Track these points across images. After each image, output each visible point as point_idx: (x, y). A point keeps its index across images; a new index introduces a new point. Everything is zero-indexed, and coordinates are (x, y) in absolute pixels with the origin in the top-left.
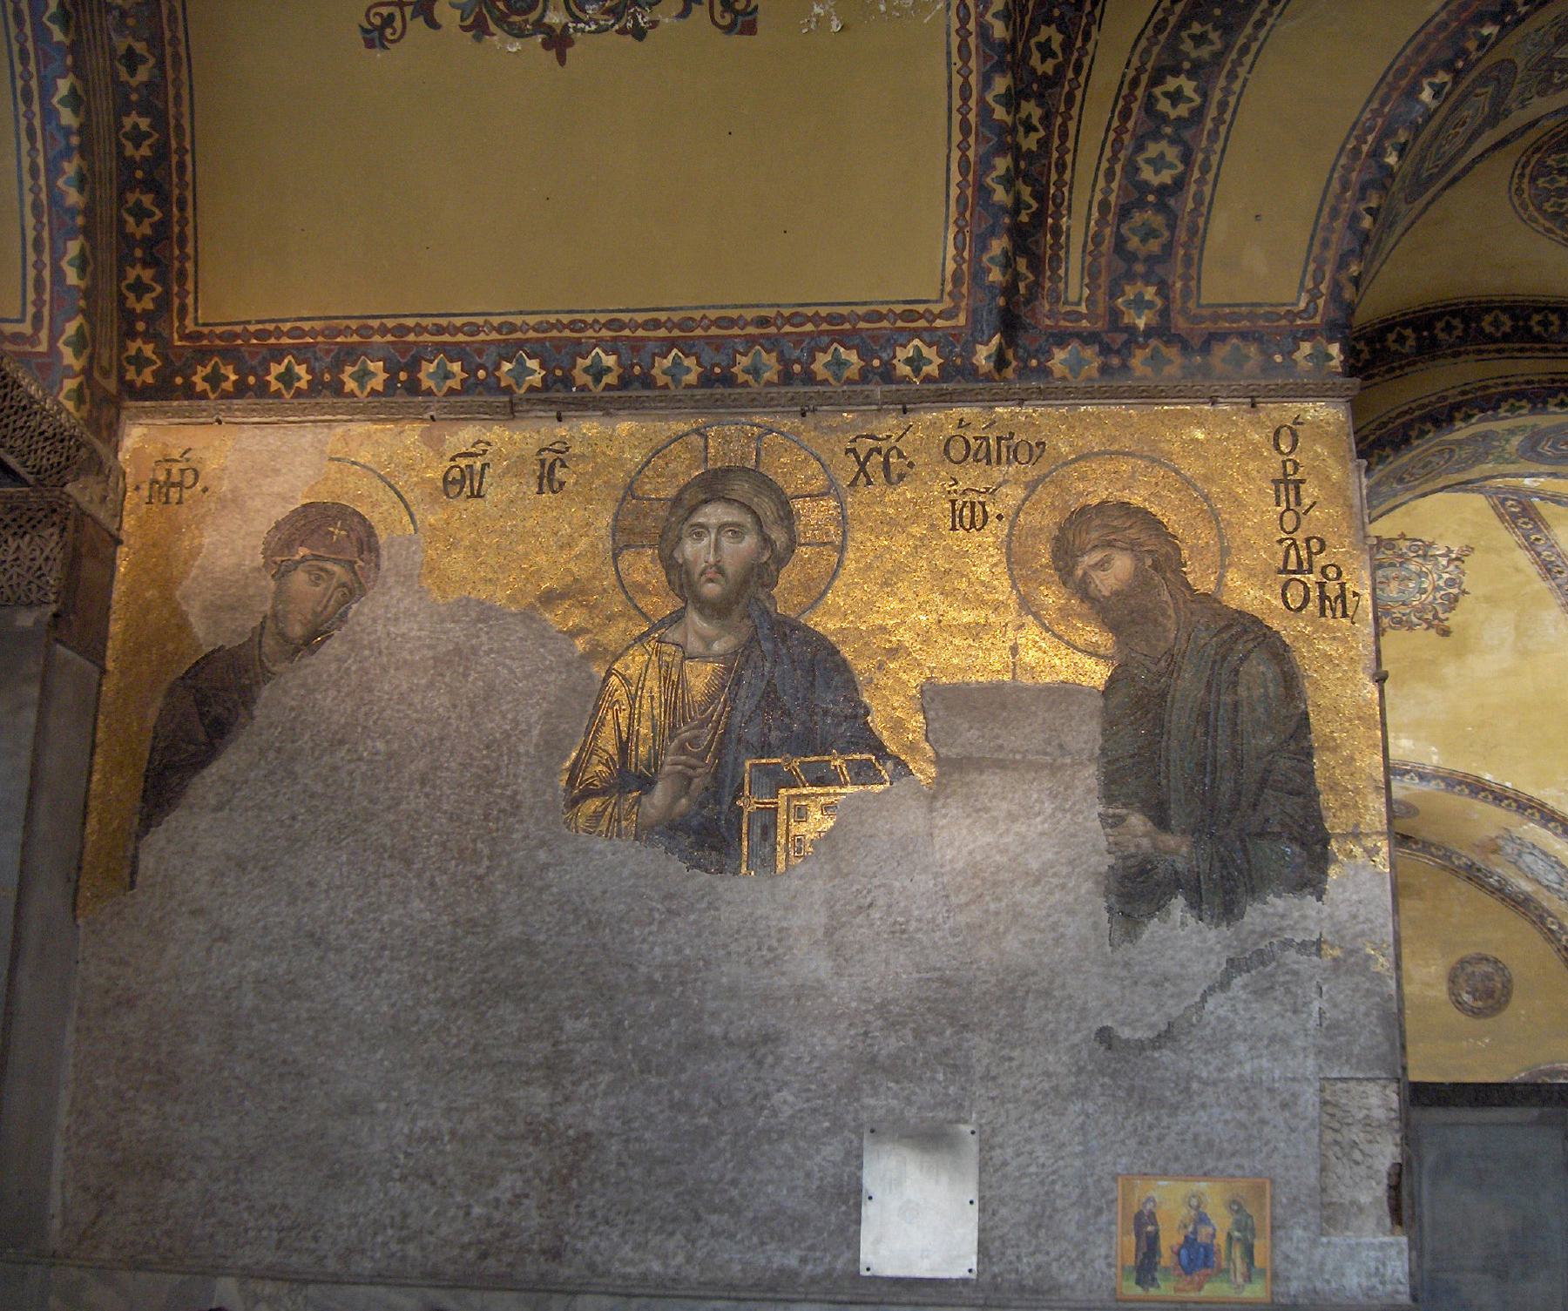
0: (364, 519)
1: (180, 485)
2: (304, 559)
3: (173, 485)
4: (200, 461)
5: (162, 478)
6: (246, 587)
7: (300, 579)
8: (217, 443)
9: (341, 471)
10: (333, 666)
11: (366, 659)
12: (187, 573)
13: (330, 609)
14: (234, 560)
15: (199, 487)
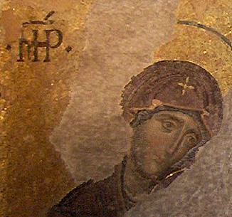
0: (210, 76)
1: (46, 44)
2: (157, 110)
3: (41, 44)
4: (63, 23)
5: (30, 39)
6: (108, 132)
7: (154, 126)
8: (77, 7)
9: (188, 33)
10: (183, 196)
11: (211, 190)
12: (57, 121)
13: (180, 151)
14: (97, 110)
15: (63, 46)
